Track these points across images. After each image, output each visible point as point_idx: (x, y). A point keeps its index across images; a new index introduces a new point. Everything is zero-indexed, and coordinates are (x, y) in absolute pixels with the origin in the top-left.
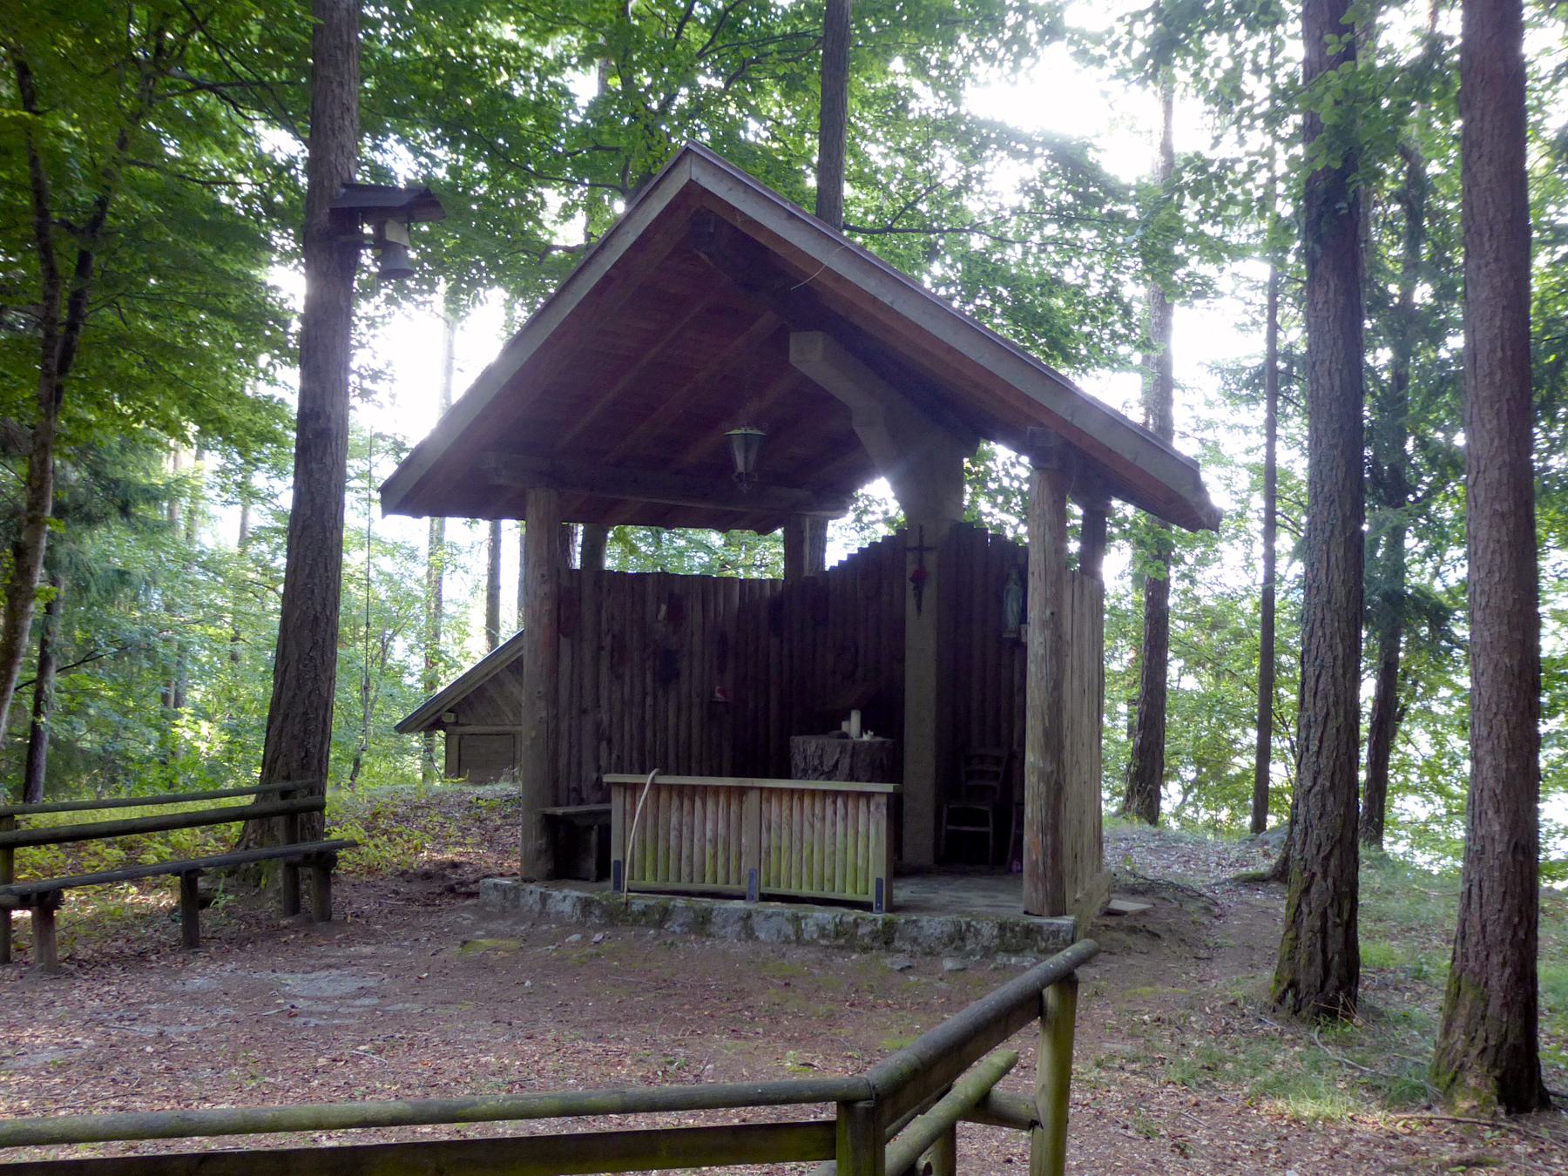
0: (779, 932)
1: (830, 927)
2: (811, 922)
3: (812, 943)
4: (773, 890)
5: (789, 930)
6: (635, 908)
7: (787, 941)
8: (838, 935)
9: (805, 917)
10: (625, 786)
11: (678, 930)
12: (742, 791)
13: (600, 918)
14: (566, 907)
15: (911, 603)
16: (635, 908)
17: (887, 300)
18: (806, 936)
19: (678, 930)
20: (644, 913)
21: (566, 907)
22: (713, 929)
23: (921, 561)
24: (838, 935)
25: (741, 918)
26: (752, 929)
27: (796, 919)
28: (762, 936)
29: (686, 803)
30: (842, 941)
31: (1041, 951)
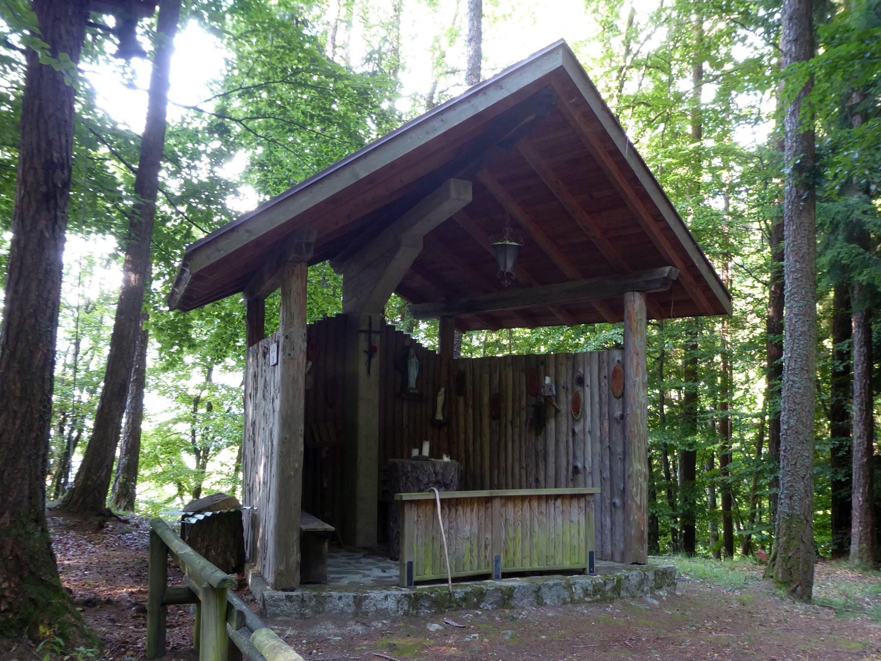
0: (559, 597)
3: (581, 601)
4: (511, 569)
5: (566, 594)
6: (457, 596)
7: (565, 603)
8: (596, 592)
9: (574, 584)
10: (417, 503)
11: (490, 607)
12: (489, 500)
13: (429, 608)
14: (391, 604)
15: (362, 368)
16: (457, 596)
17: (638, 176)
18: (576, 597)
19: (490, 607)
20: (464, 599)
21: (391, 604)
22: (513, 603)
23: (370, 340)
24: (596, 592)
25: (535, 592)
26: (542, 598)
27: (569, 586)
28: (548, 602)
29: (453, 510)
31: (668, 586)
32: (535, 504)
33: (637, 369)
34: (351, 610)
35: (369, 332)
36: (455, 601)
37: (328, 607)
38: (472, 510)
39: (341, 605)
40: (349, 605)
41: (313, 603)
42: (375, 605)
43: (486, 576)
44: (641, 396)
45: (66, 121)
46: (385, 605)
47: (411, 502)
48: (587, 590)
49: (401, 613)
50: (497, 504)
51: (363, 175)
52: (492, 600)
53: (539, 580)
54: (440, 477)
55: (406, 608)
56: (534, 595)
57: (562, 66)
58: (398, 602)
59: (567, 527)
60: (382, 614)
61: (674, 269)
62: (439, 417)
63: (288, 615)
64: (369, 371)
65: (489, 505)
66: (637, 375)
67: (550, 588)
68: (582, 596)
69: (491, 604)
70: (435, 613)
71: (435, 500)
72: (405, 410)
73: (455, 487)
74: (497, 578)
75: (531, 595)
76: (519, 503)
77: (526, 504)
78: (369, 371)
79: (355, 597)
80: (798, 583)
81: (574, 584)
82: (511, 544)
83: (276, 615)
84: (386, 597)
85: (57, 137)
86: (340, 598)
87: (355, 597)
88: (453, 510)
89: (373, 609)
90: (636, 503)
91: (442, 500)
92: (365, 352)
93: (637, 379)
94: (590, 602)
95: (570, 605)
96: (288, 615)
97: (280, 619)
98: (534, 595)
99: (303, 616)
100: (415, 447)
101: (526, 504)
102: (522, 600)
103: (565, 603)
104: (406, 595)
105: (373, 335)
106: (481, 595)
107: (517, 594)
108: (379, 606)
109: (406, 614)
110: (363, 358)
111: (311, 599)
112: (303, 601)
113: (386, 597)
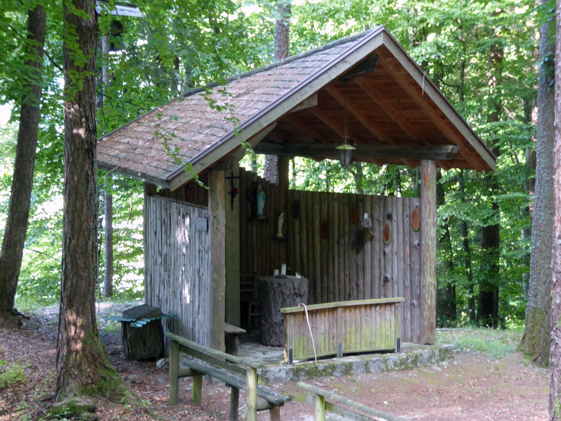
0: (379, 368)
1: (398, 362)
2: (391, 361)
3: (392, 370)
4: (348, 351)
5: (383, 366)
6: (320, 369)
7: (383, 371)
8: (401, 364)
9: (388, 359)
10: (294, 314)
11: (339, 375)
12: (334, 309)
13: (305, 376)
14: (283, 374)
16: (320, 369)
18: (390, 368)
19: (339, 375)
20: (324, 370)
21: (283, 374)
22: (352, 372)
25: (365, 365)
27: (385, 361)
28: (373, 371)
30: (403, 366)
31: (449, 358)
36: (319, 372)
38: (325, 316)
42: (274, 375)
43: (334, 356)
44: (432, 232)
46: (279, 375)
47: (291, 314)
49: (289, 379)
50: (340, 311)
52: (340, 370)
53: (367, 357)
54: (297, 291)
55: (291, 376)
56: (364, 367)
58: (287, 373)
59: (383, 324)
60: (278, 380)
61: (455, 147)
62: (280, 235)
65: (335, 312)
66: (429, 218)
67: (374, 362)
69: (339, 373)
70: (308, 379)
72: (255, 231)
74: (340, 356)
76: (353, 310)
80: (538, 354)
81: (388, 359)
82: (348, 336)
84: (280, 370)
88: (314, 317)
90: (428, 305)
91: (308, 311)
92: (229, 193)
93: (429, 220)
94: (398, 370)
95: (386, 373)
97: (220, 384)
104: (291, 369)
105: (234, 180)
106: (334, 368)
107: (354, 367)
108: (276, 376)
109: (292, 380)
113: (280, 370)
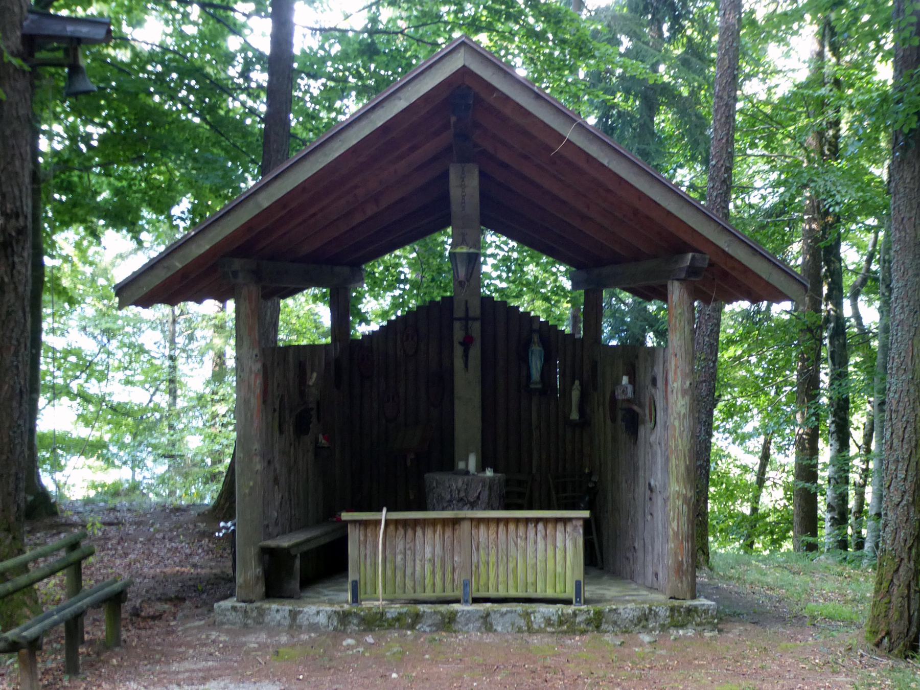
0: (513, 624)
1: (555, 618)
2: (538, 615)
3: (539, 631)
4: (482, 594)
5: (522, 623)
6: (389, 616)
7: (520, 630)
8: (561, 623)
9: (534, 612)
11: (428, 629)
12: (455, 522)
13: (358, 625)
14: (322, 619)
15: (458, 363)
16: (389, 616)
17: (605, 162)
18: (535, 626)
19: (428, 629)
21: (322, 619)
23: (466, 329)
26: (491, 625)
27: (527, 615)
28: (499, 629)
29: (410, 532)
30: (565, 627)
31: (698, 625)
32: (512, 527)
33: (675, 373)
34: (287, 623)
35: (467, 319)
36: (387, 620)
37: (267, 619)
38: (435, 532)
39: (278, 617)
40: (285, 618)
41: (255, 614)
42: (308, 619)
43: (457, 601)
44: (679, 405)
45: (17, 173)
46: (316, 619)
47: (354, 522)
48: (550, 619)
49: (331, 628)
50: (466, 526)
51: (266, 204)
52: (430, 622)
53: (530, 607)
54: (462, 494)
55: (335, 624)
56: (481, 620)
57: (464, 66)
58: (329, 618)
59: (550, 553)
60: (314, 627)
61: (697, 255)
62: (575, 416)
63: (234, 624)
64: (466, 366)
65: (457, 527)
66: (675, 380)
67: (503, 615)
68: (543, 626)
69: (429, 626)
70: (364, 630)
71: (380, 521)
72: (534, 409)
73: (483, 506)
74: (466, 602)
75: (477, 620)
76: (493, 527)
77: (502, 527)
78: (466, 366)
79: (290, 611)
80: (883, 634)
81: (534, 612)
82: (482, 569)
83: (223, 623)
84: (318, 613)
85: (10, 189)
86: (278, 611)
87: (290, 611)
88: (410, 532)
89: (306, 623)
90: (673, 530)
91: (386, 521)
92: (460, 343)
93: (675, 385)
94: (553, 633)
95: (526, 634)
96: (234, 624)
97: (226, 627)
98: (481, 620)
99: (246, 625)
100: (461, 460)
101: (502, 527)
102: (467, 624)
103: (520, 630)
104: (335, 612)
105: (470, 322)
106: (417, 617)
107: (460, 619)
108: (311, 621)
109: (335, 629)
110: (458, 351)
111: (252, 610)
112: (246, 612)
113: (318, 613)
